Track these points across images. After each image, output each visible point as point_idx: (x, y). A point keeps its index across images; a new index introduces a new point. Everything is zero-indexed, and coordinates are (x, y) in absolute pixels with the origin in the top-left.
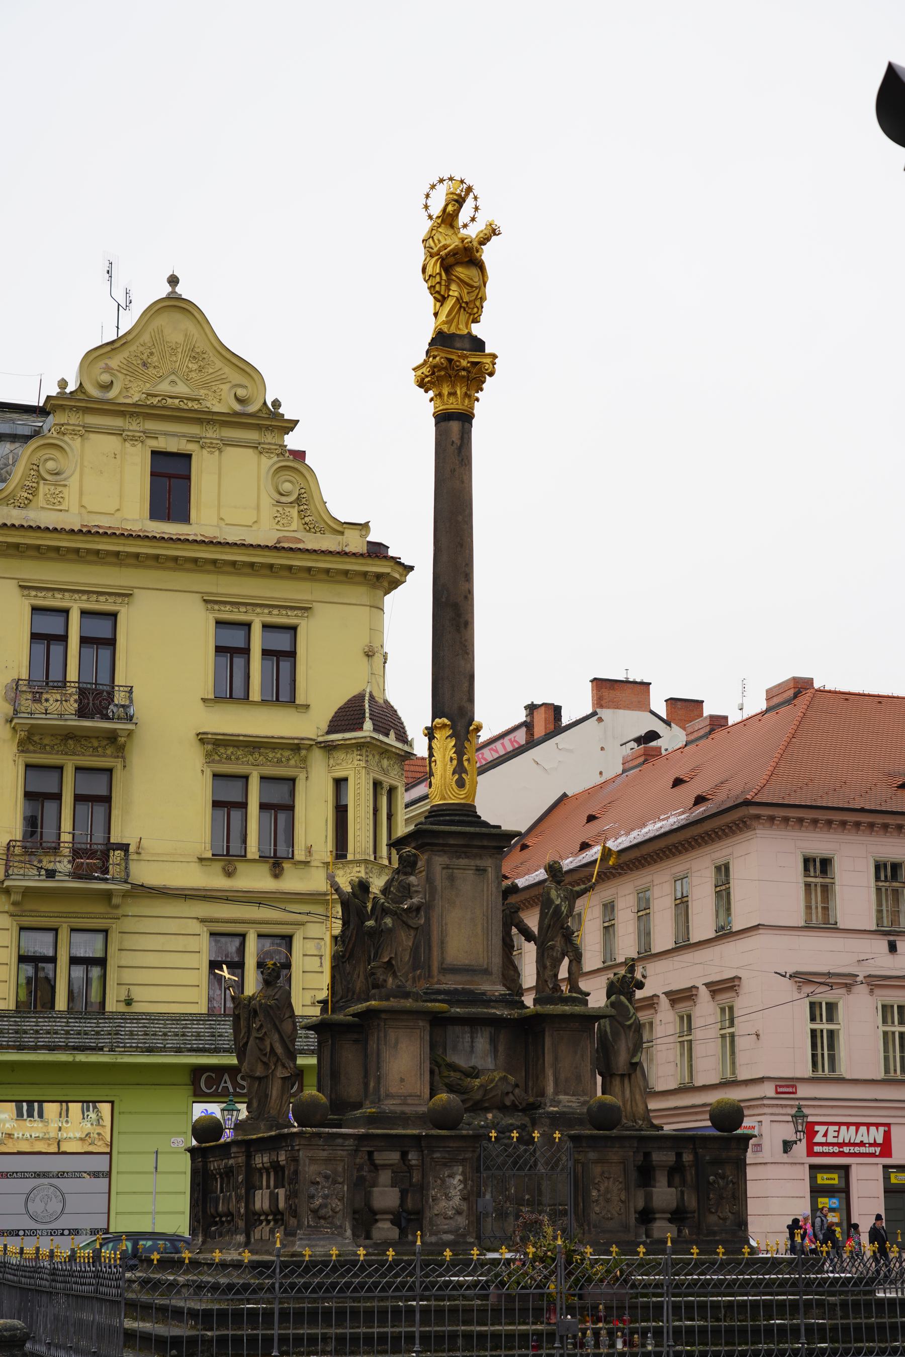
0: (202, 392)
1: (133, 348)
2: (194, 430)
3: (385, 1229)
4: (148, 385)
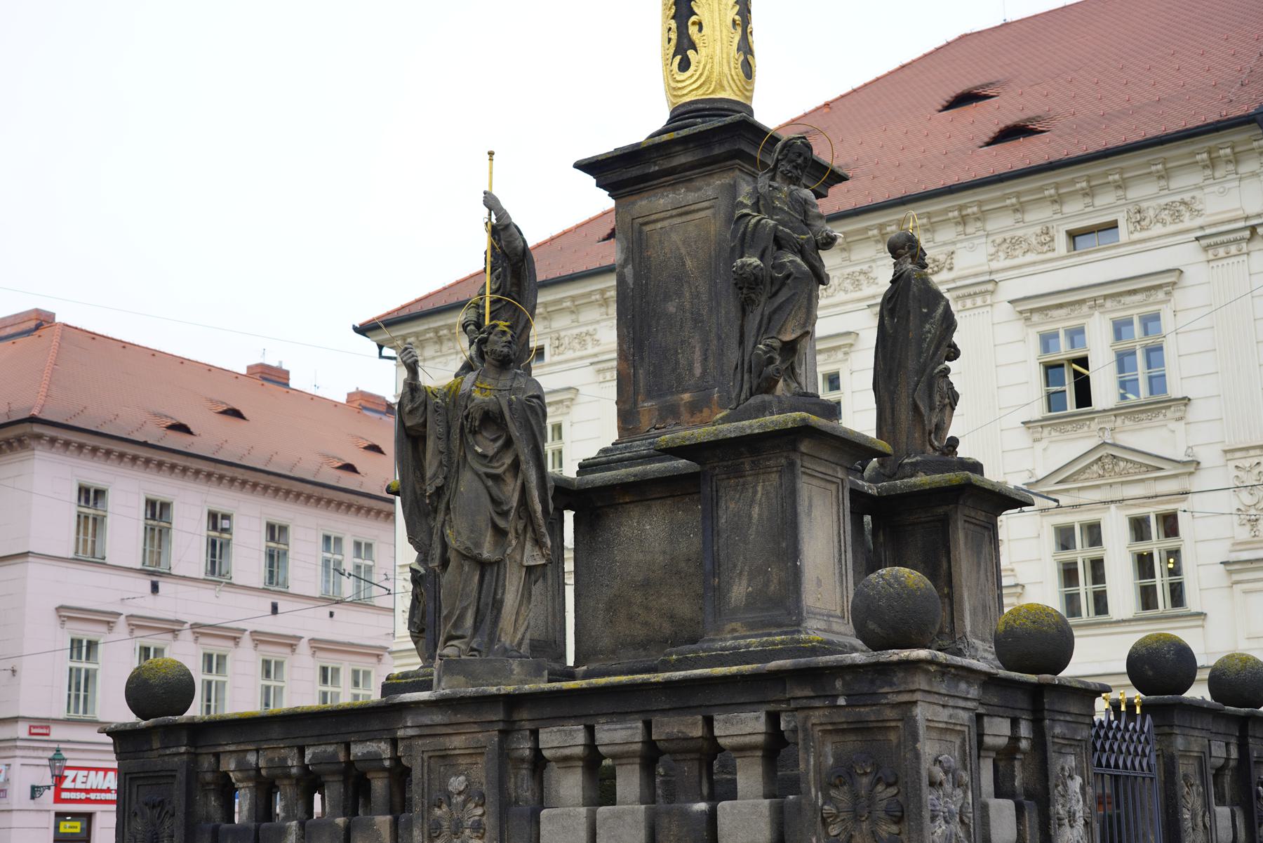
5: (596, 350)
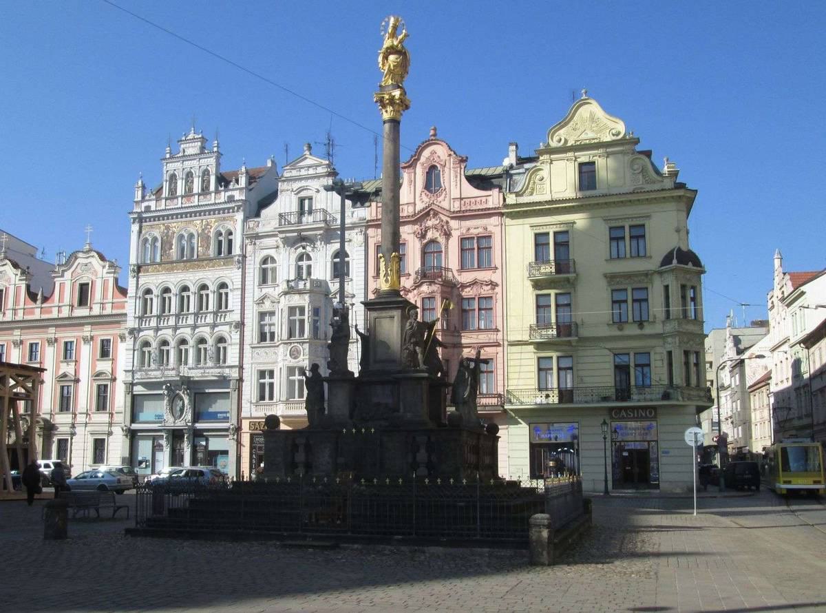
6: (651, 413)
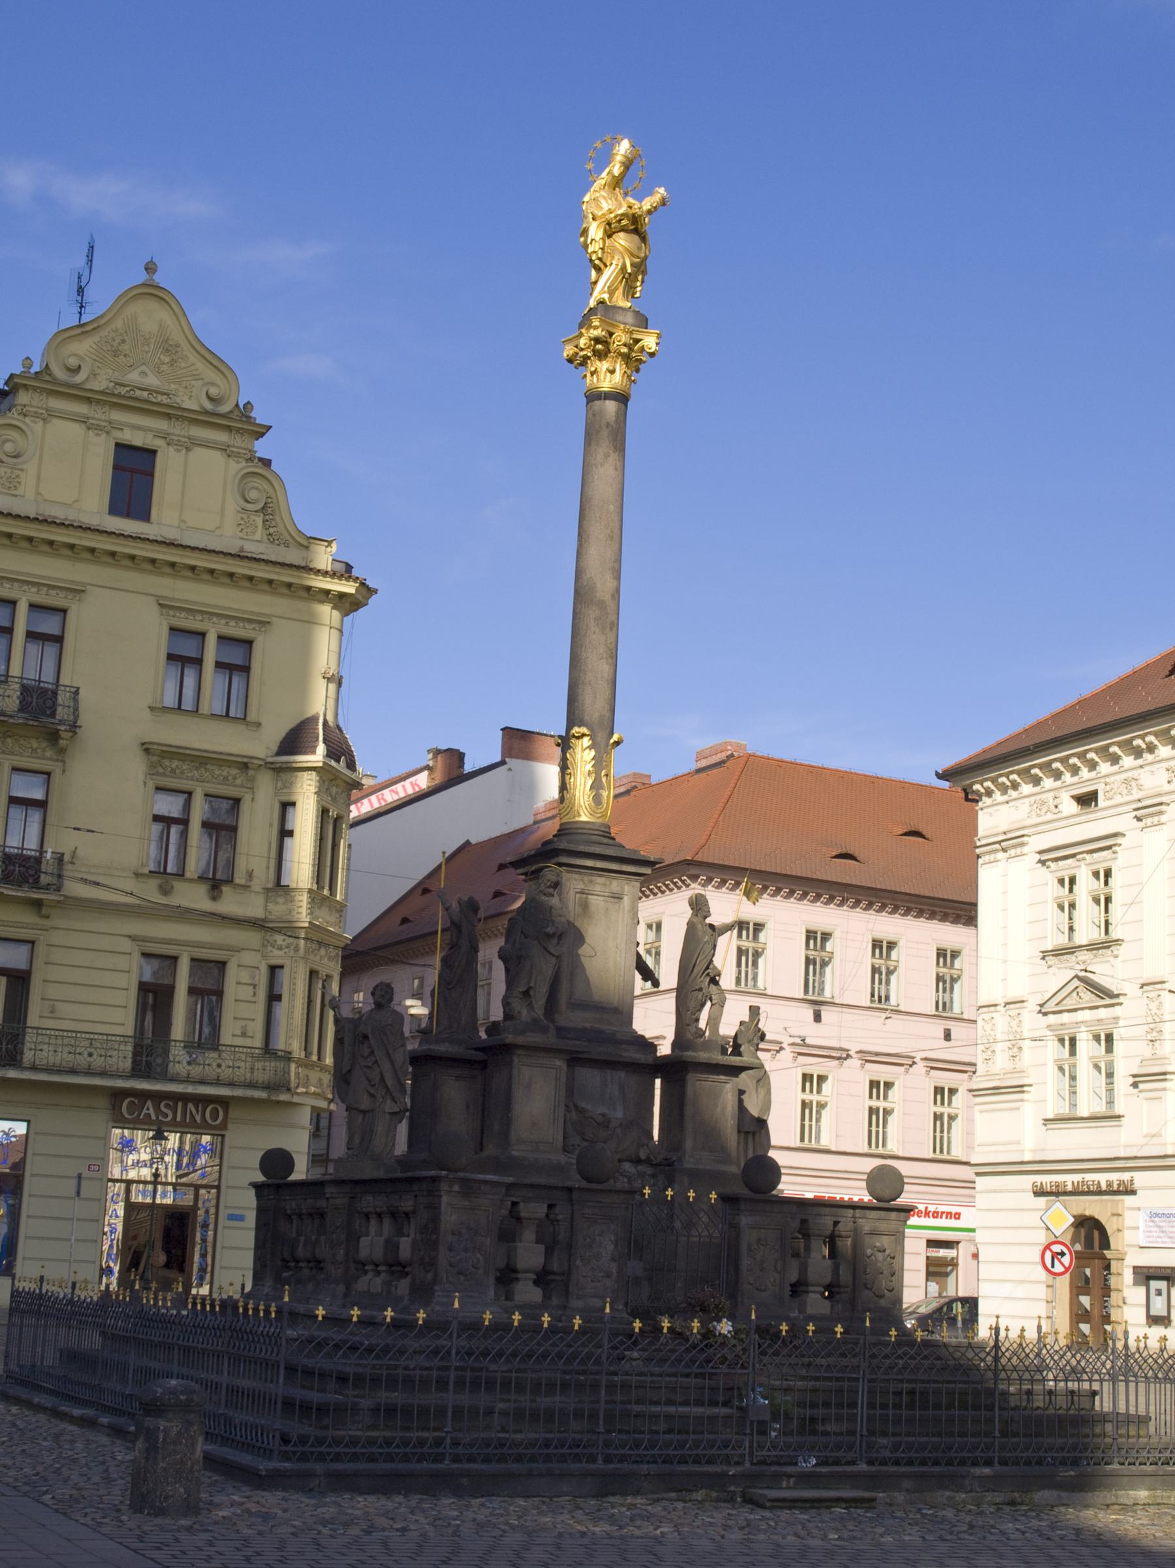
0: (173, 386)
1: (104, 333)
2: (162, 425)
3: (527, 1292)
4: (116, 374)
5: (1140, 795)
6: (215, 1115)
